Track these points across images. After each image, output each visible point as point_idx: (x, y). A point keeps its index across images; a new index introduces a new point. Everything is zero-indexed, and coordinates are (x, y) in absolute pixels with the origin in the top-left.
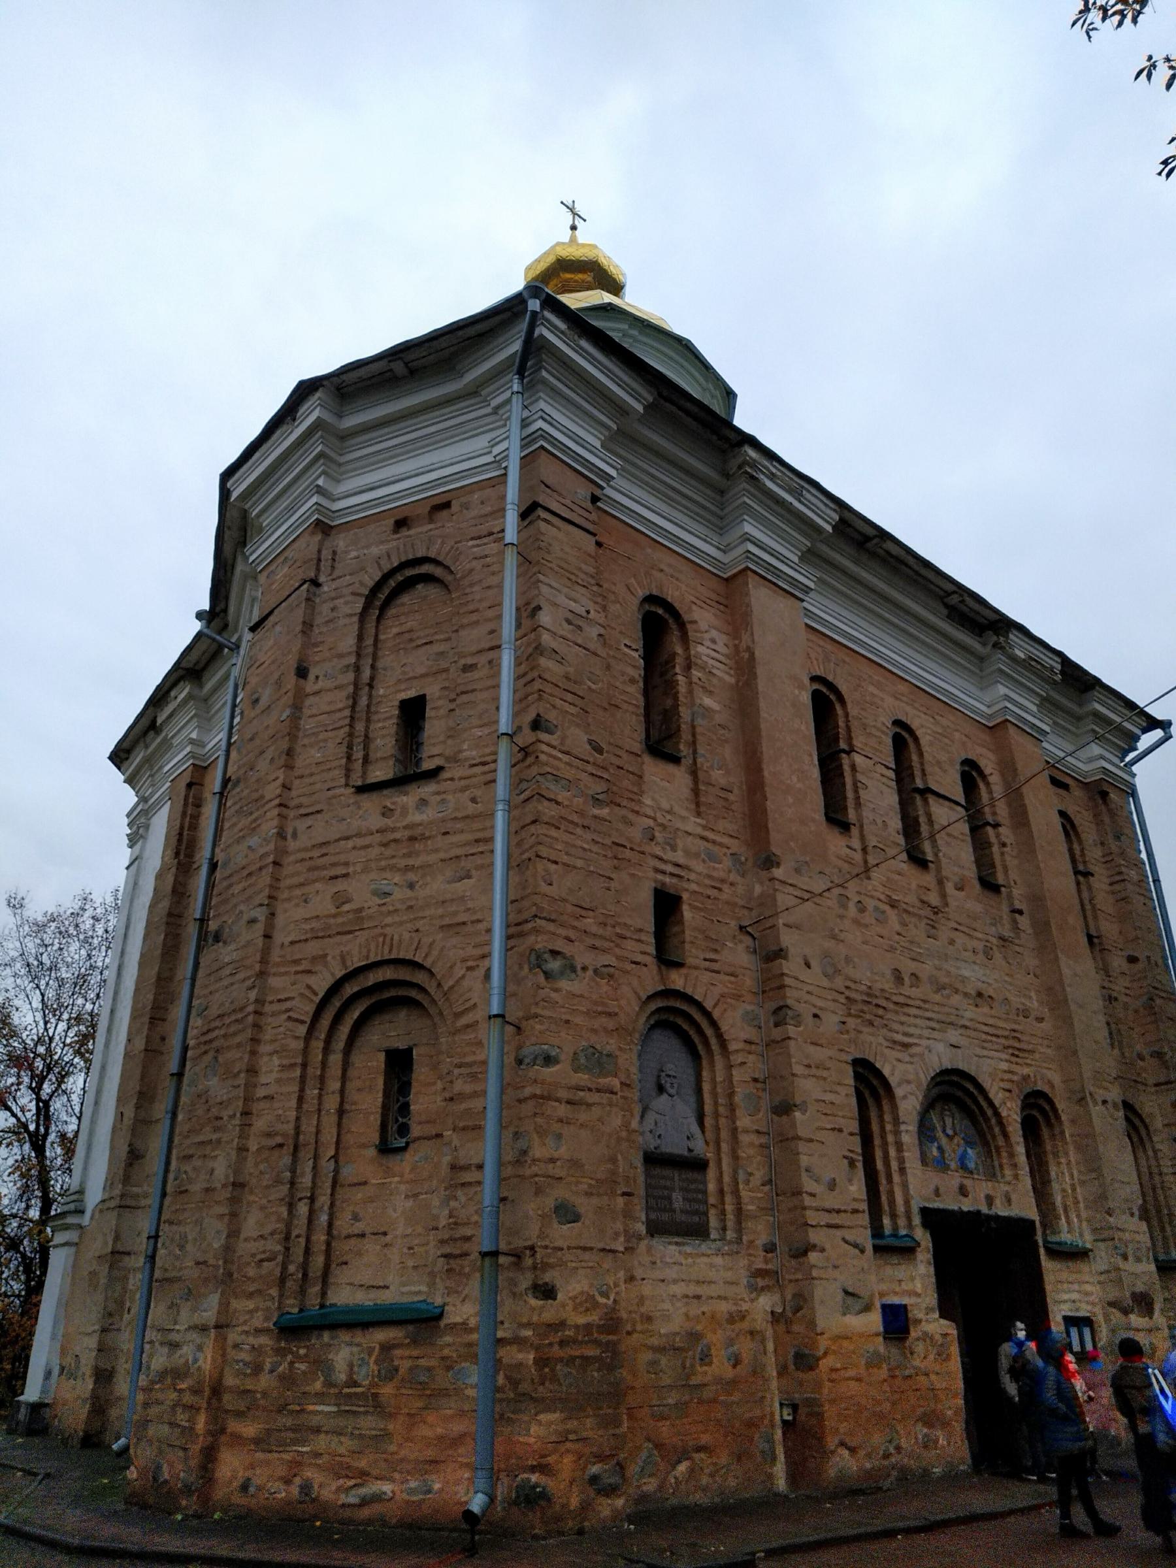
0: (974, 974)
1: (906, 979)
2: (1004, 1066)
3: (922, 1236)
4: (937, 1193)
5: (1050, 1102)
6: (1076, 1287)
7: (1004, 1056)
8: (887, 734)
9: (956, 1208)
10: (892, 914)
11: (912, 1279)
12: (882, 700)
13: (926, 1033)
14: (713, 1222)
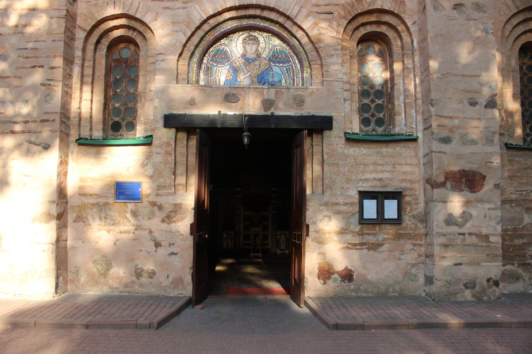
5: (397, 16)
6: (390, 168)
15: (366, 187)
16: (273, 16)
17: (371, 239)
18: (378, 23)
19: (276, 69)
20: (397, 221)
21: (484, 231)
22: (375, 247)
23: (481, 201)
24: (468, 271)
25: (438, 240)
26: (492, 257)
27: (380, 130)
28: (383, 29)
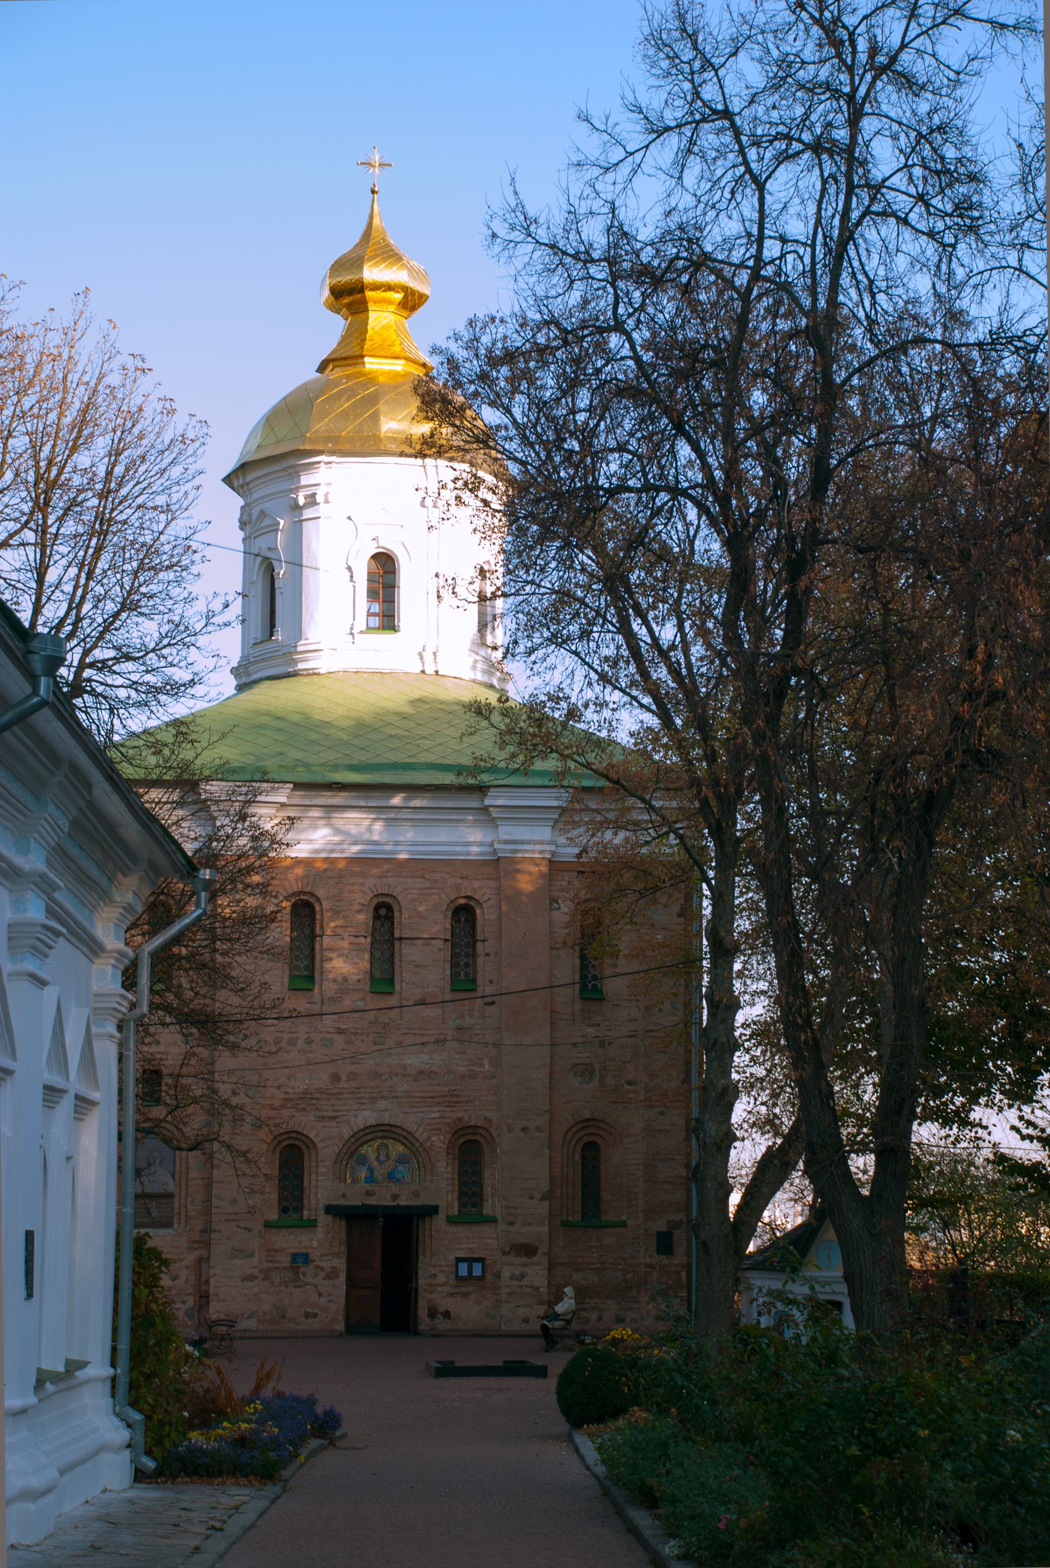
0: (415, 1060)
1: (344, 1077)
2: (437, 1115)
3: (324, 1219)
4: (344, 1196)
7: (434, 1109)
8: (359, 911)
9: (359, 1203)
10: (340, 1039)
11: (311, 1240)
12: (363, 885)
13: (355, 1107)
14: (176, 1220)
15: (462, 1255)
16: (399, 1131)
17: (463, 1289)
18: (474, 1134)
19: (401, 1168)
20: (482, 1278)
21: (536, 1284)
22: (466, 1295)
23: (535, 1264)
24: (524, 1312)
25: (504, 1290)
26: (540, 1303)
27: (474, 1210)
28: (478, 1137)
